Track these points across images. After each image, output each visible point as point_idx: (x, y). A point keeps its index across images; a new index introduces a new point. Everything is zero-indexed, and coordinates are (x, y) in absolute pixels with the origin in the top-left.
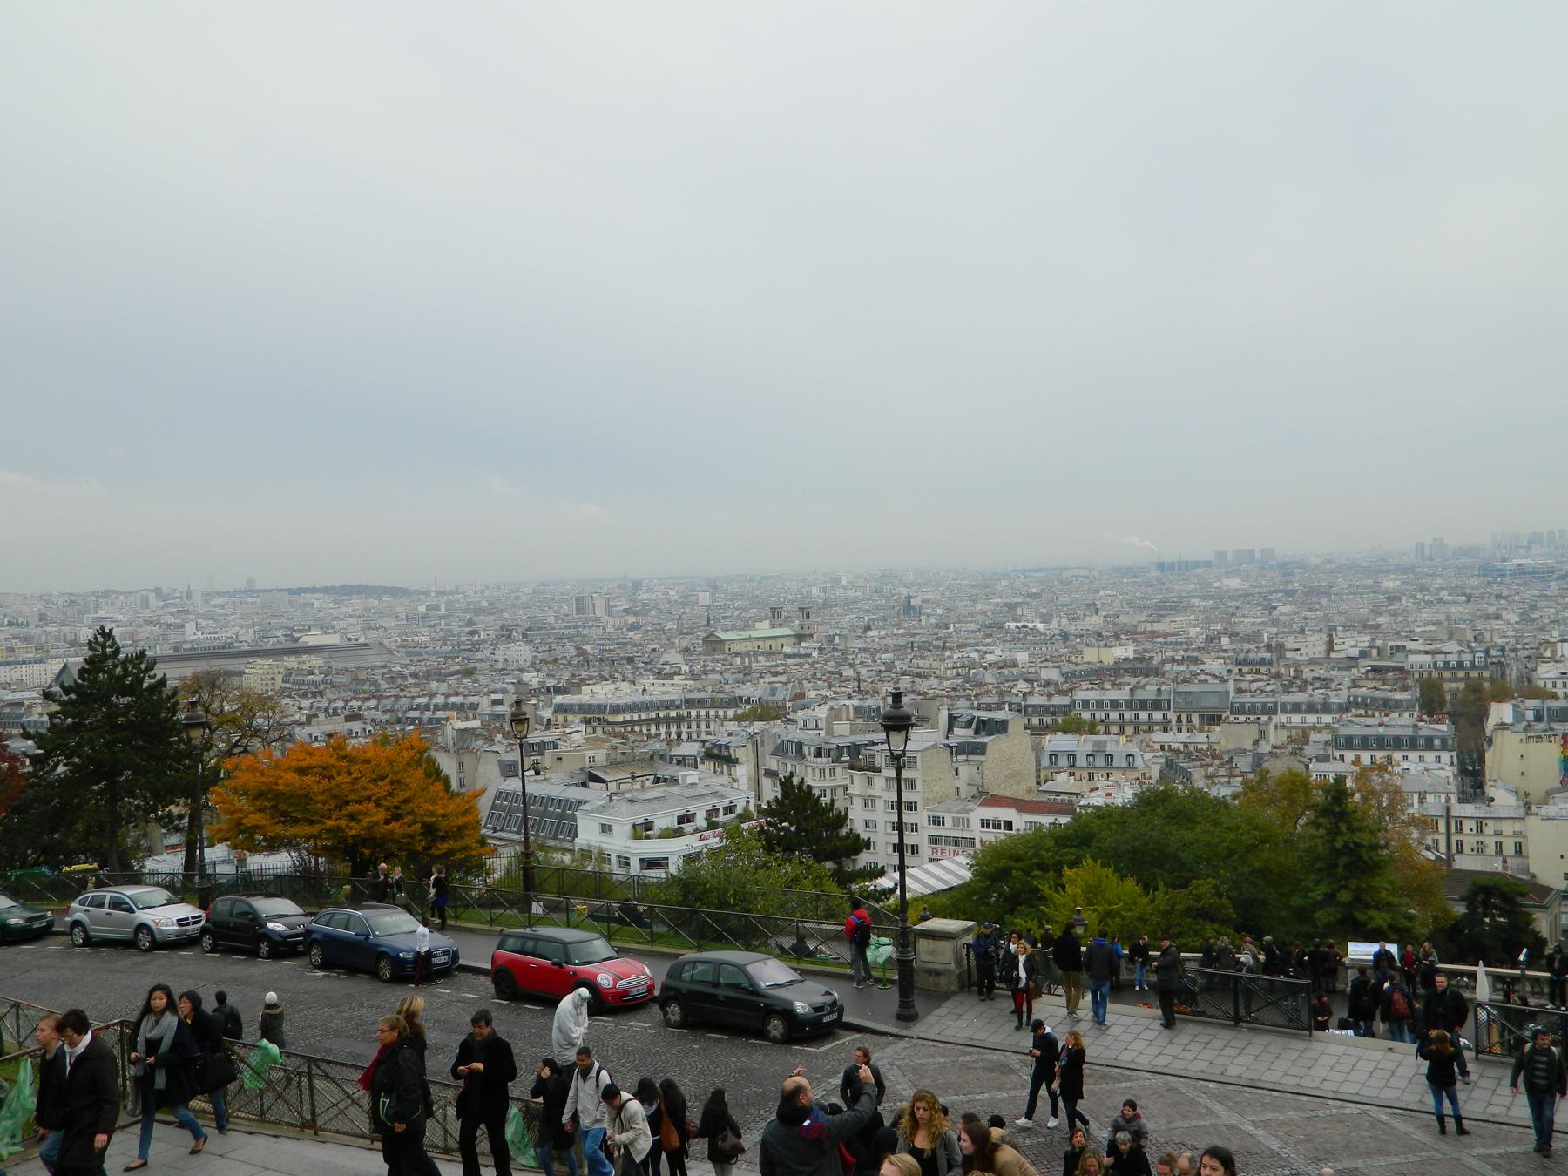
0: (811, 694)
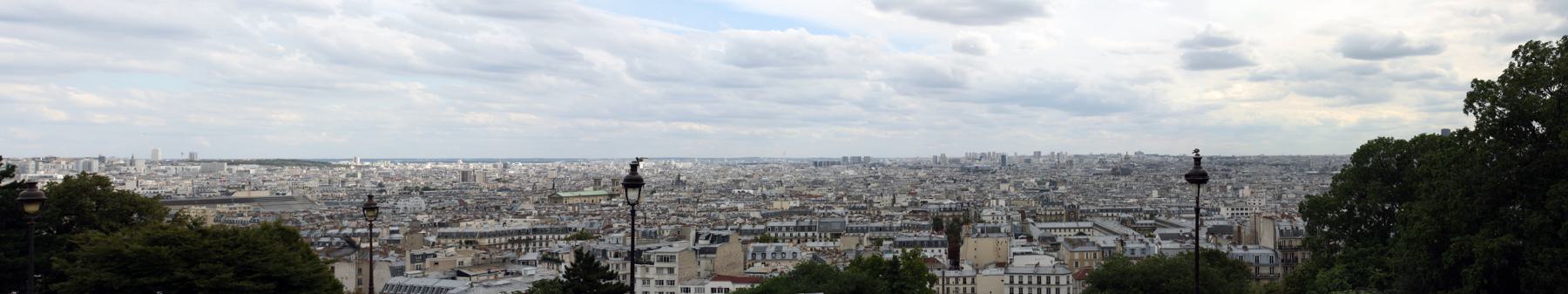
0: (616, 226)
